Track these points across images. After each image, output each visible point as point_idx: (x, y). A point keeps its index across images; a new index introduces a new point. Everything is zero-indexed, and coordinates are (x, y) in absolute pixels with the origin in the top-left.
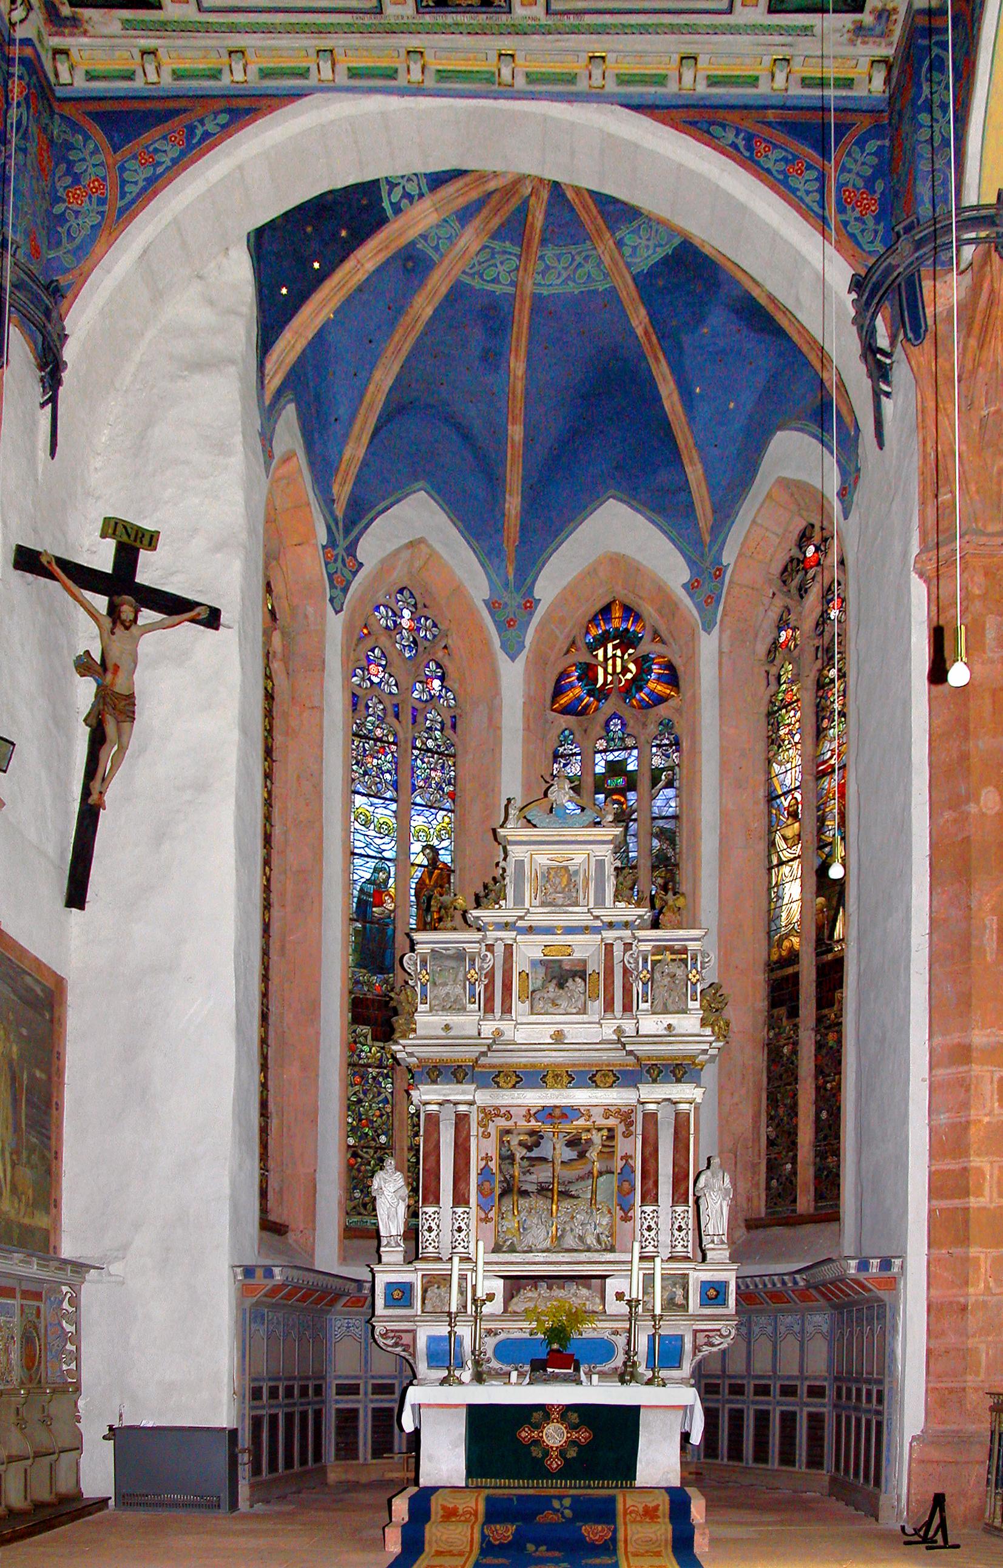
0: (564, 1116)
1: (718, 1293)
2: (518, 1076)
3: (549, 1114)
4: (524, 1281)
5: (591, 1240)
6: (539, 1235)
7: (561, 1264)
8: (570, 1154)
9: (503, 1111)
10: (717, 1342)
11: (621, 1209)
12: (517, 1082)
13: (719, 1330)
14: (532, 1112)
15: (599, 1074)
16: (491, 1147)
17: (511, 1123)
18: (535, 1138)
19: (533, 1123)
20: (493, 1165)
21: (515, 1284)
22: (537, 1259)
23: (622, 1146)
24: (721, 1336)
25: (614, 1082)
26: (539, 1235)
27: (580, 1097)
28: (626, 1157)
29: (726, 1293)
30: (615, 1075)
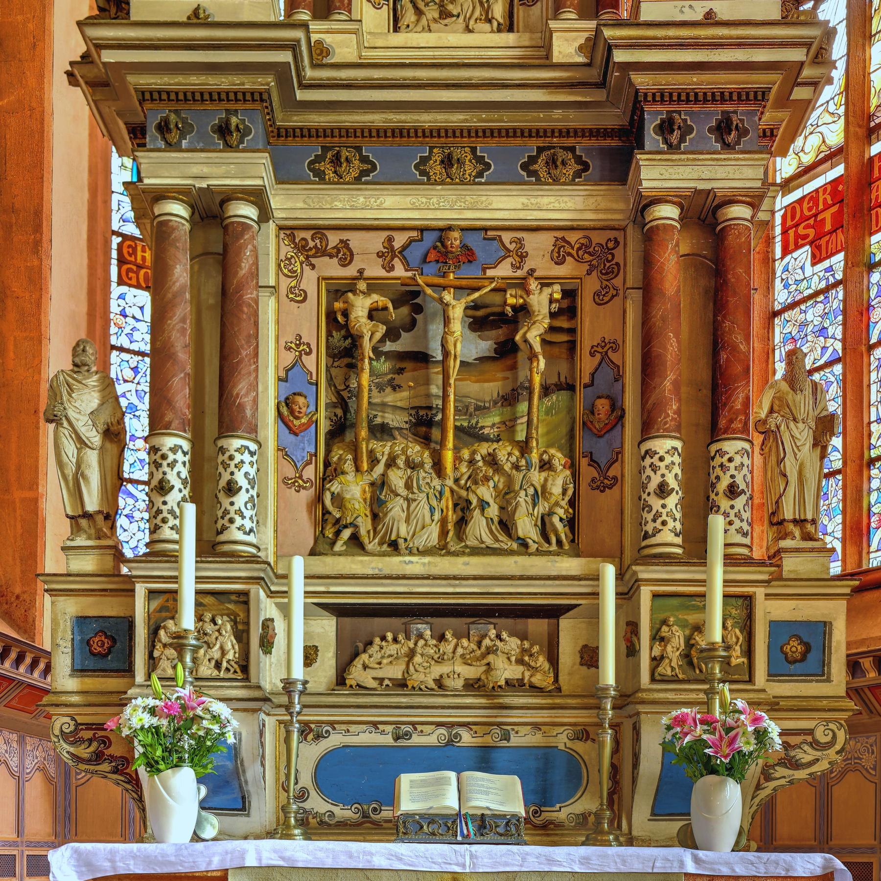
0: (468, 255)
1: (808, 648)
2: (364, 160)
4: (378, 622)
5: (526, 527)
7: (466, 574)
8: (479, 346)
9: (333, 239)
10: (807, 759)
11: (593, 462)
12: (364, 173)
13: (811, 732)
14: (397, 244)
15: (543, 157)
17: (350, 271)
18: (405, 310)
19: (400, 271)
20: (310, 362)
22: (410, 570)
24: (815, 744)
25: (578, 174)
26: (417, 515)
27: (503, 204)
28: (607, 349)
29: (825, 648)
30: (579, 160)
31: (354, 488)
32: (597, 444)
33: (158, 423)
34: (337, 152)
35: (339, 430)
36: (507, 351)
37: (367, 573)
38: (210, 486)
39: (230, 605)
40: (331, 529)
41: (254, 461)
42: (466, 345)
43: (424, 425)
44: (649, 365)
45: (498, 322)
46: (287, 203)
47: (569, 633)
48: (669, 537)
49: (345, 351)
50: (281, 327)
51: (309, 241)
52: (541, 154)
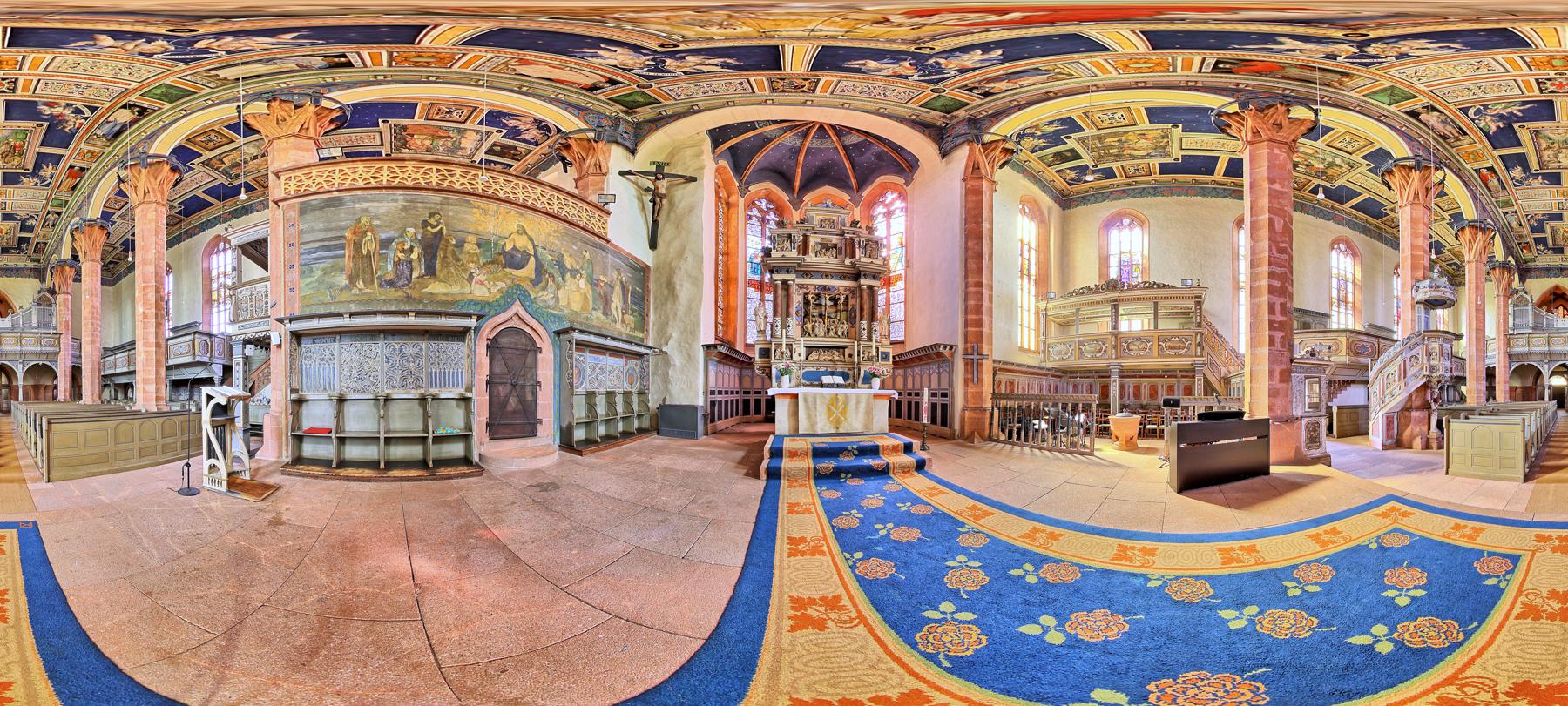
3: (824, 288)
6: (820, 330)
16: (800, 298)
21: (810, 349)
23: (851, 301)
26: (820, 330)
31: (809, 326)
32: (851, 320)
33: (775, 315)
34: (807, 274)
35: (806, 315)
36: (836, 304)
37: (813, 341)
38: (785, 326)
39: (790, 346)
40: (805, 333)
41: (793, 321)
42: (829, 303)
43: (821, 316)
44: (862, 310)
45: (835, 300)
46: (799, 281)
47: (847, 352)
48: (865, 336)
49: (807, 302)
50: (797, 299)
51: (801, 286)
52: (843, 276)
